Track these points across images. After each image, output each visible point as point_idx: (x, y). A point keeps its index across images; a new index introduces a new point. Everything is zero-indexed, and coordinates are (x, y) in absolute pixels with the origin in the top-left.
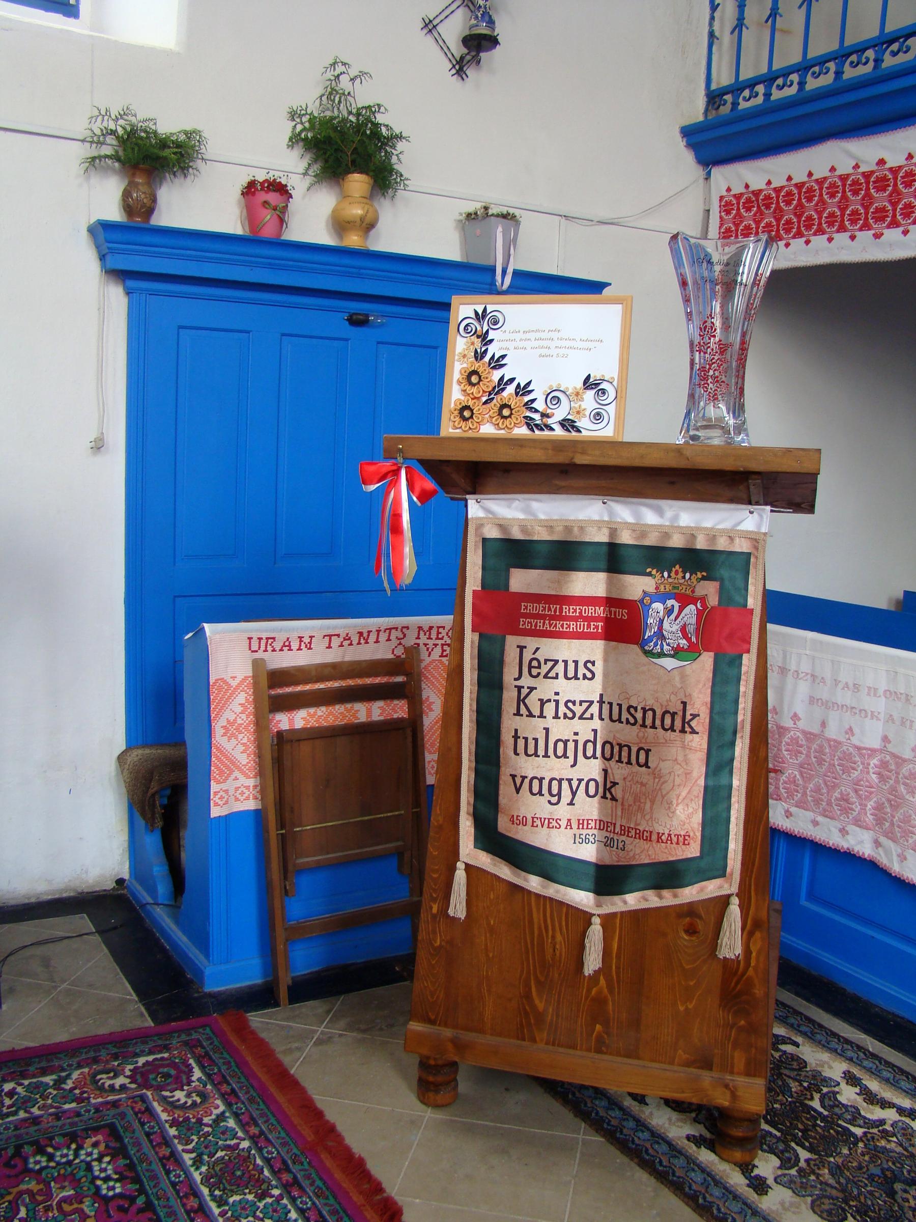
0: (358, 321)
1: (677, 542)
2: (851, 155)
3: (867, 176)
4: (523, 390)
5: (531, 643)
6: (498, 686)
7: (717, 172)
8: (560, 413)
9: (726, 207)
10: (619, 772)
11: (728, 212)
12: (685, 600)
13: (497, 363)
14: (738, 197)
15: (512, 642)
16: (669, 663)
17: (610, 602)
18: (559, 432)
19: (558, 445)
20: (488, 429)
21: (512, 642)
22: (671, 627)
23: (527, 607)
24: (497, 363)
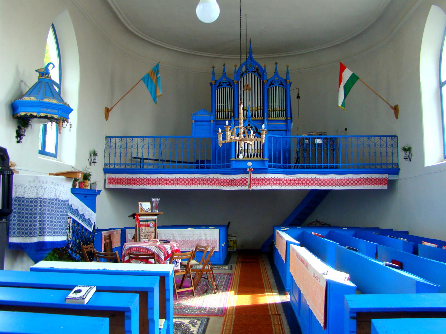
0: (86, 197)
1: (152, 219)
2: (128, 176)
3: (131, 179)
4: (144, 209)
5: (142, 228)
6: (140, 231)
7: (106, 174)
8: (147, 211)
9: (109, 179)
10: (148, 237)
11: (109, 180)
12: (152, 223)
13: (142, 207)
14: (111, 178)
15: (141, 228)
16: (152, 228)
17: (146, 224)
18: (147, 212)
19: (148, 213)
20: (143, 212)
21: (141, 228)
22: (152, 225)
23: (142, 225)
24: (142, 207)
